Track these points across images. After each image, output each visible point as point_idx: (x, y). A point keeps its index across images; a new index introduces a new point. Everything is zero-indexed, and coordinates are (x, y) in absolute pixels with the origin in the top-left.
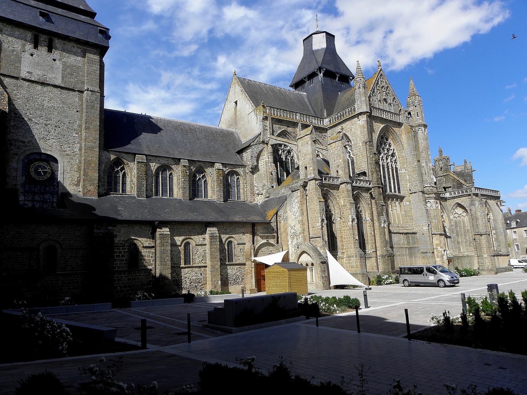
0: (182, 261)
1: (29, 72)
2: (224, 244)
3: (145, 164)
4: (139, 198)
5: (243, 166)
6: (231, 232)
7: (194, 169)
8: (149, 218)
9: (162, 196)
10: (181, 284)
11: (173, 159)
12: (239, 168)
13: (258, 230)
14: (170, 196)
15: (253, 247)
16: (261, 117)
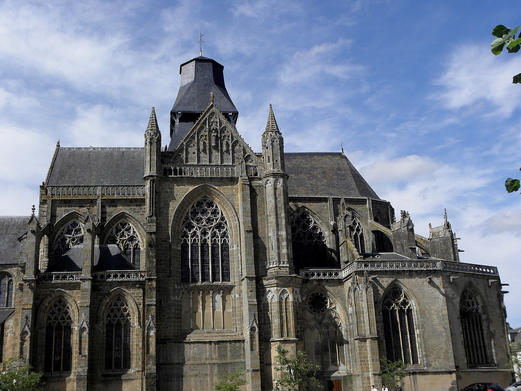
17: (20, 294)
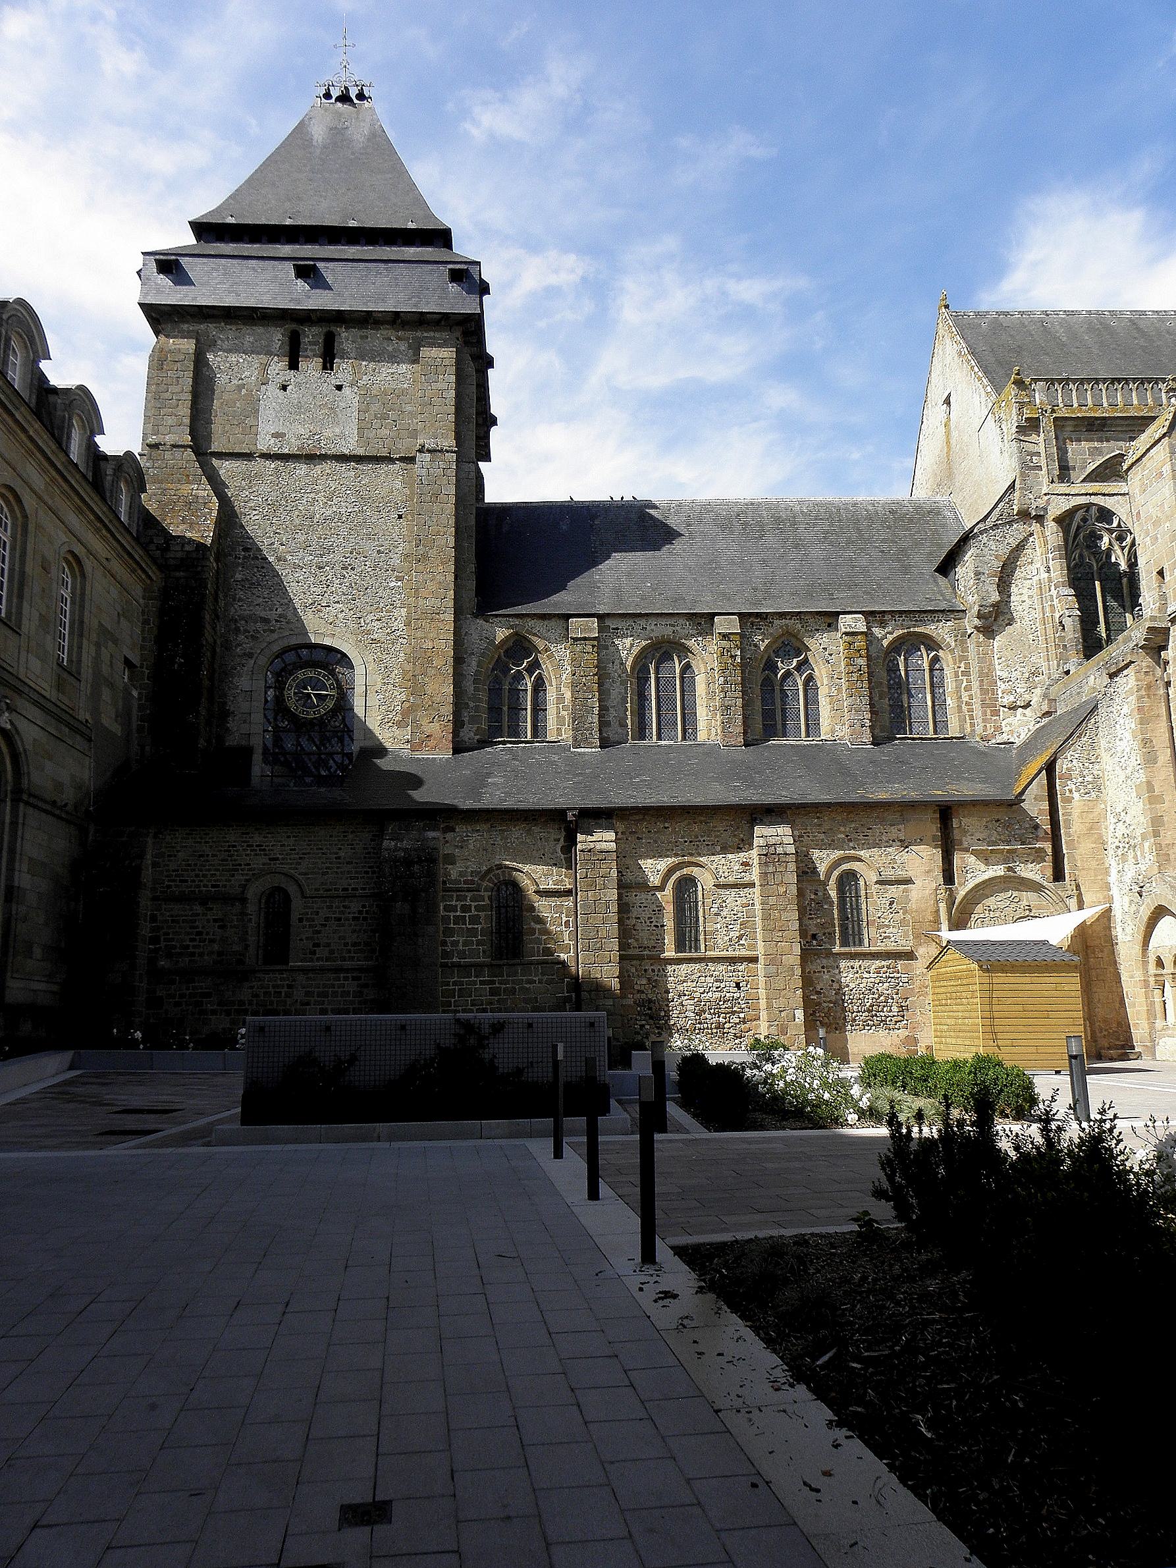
0: (669, 940)
1: (276, 435)
2: (825, 884)
3: (596, 643)
4: (579, 750)
5: (953, 611)
6: (850, 840)
7: (767, 642)
8: (558, 801)
9: (659, 738)
10: (665, 1016)
11: (691, 616)
12: (937, 621)
13: (965, 832)
14: (684, 738)
15: (942, 893)
16: (1010, 428)
17: (1144, 664)
